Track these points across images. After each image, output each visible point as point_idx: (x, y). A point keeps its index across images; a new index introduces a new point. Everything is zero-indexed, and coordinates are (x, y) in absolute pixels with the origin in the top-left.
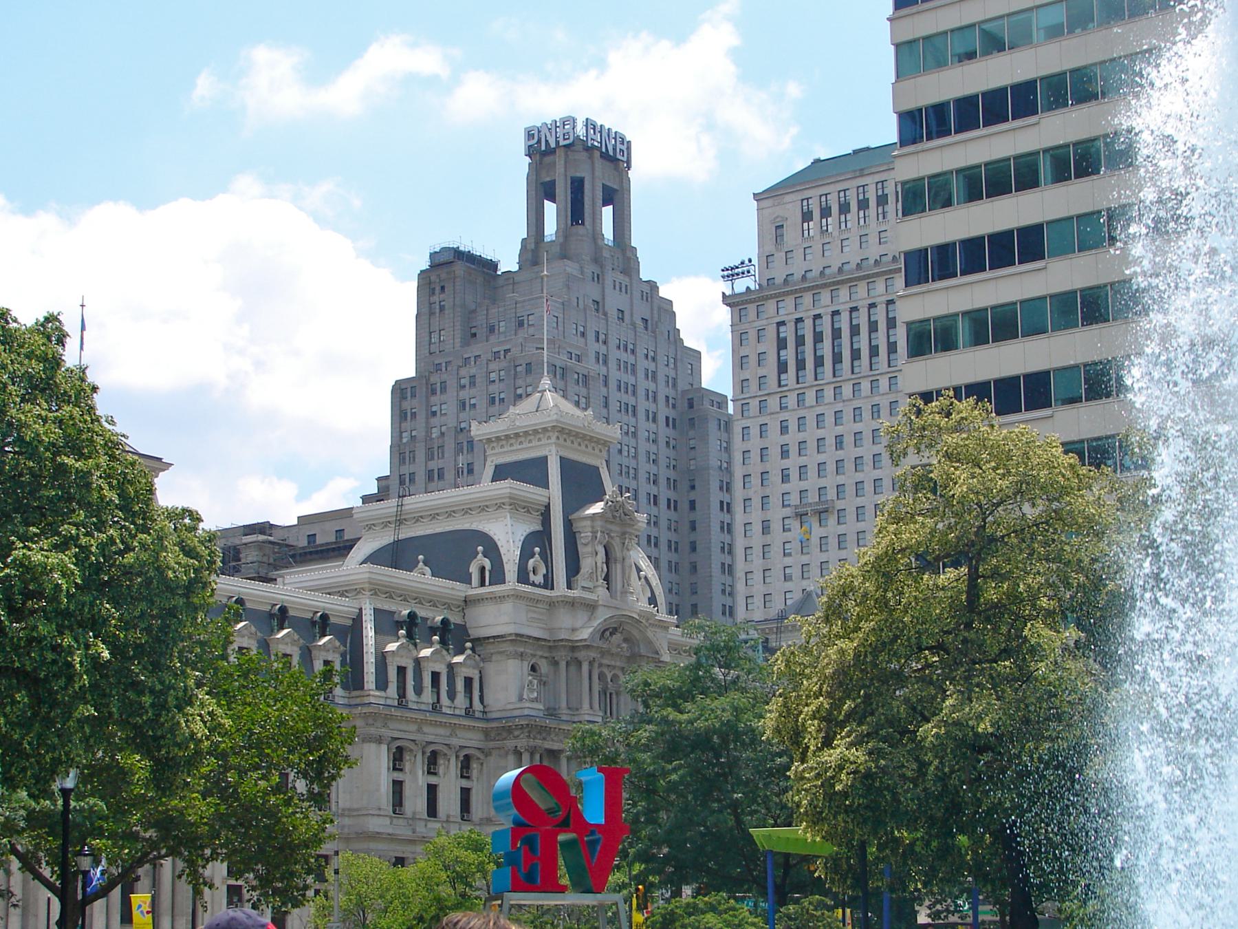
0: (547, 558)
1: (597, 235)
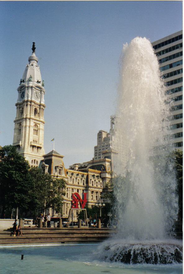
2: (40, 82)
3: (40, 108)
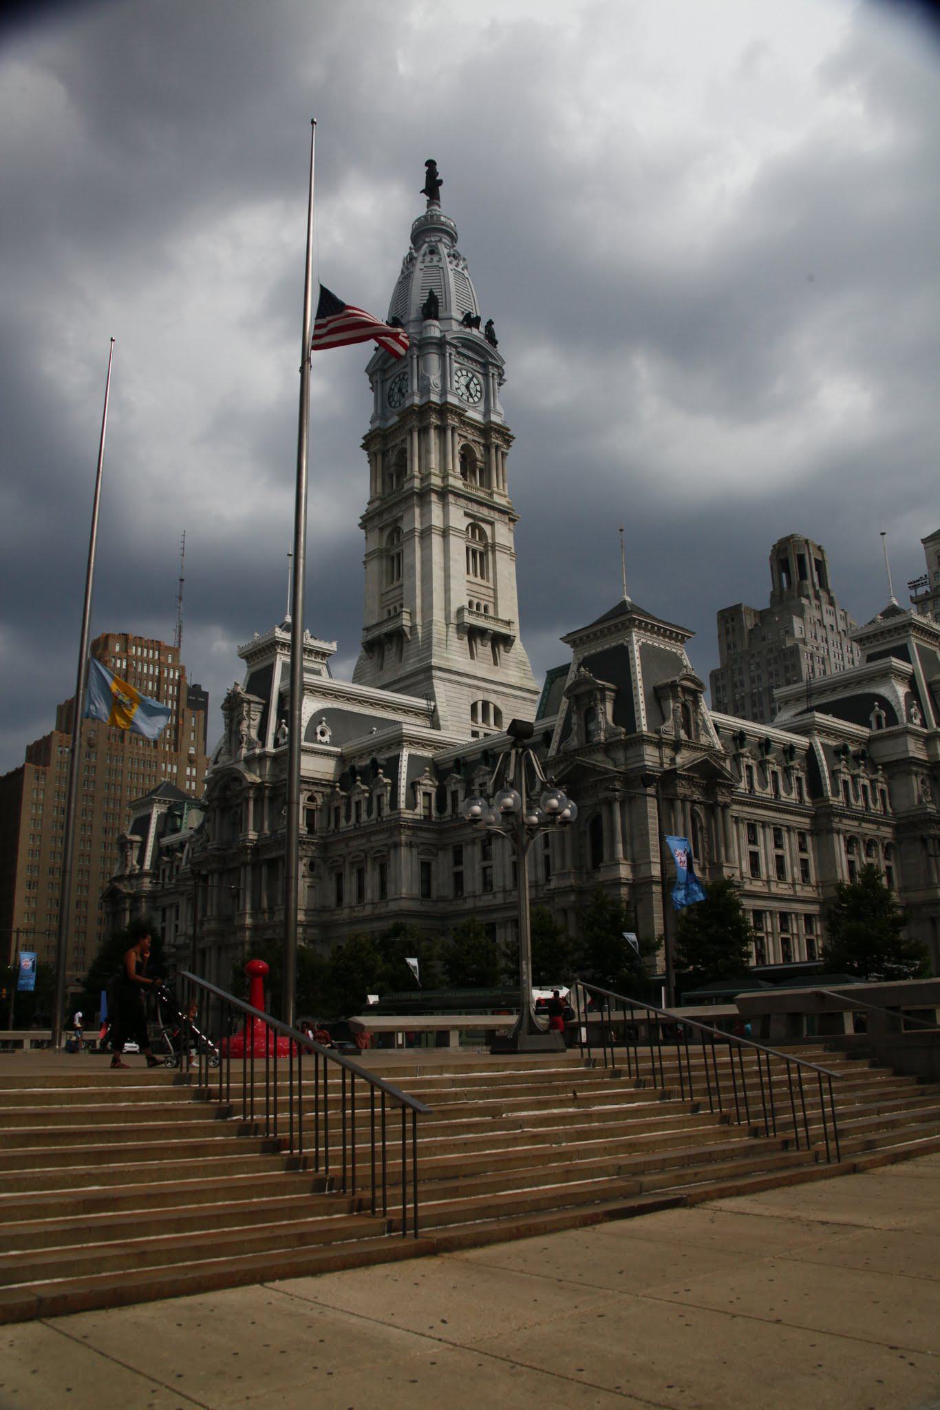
2: (478, 319)
3: (487, 448)
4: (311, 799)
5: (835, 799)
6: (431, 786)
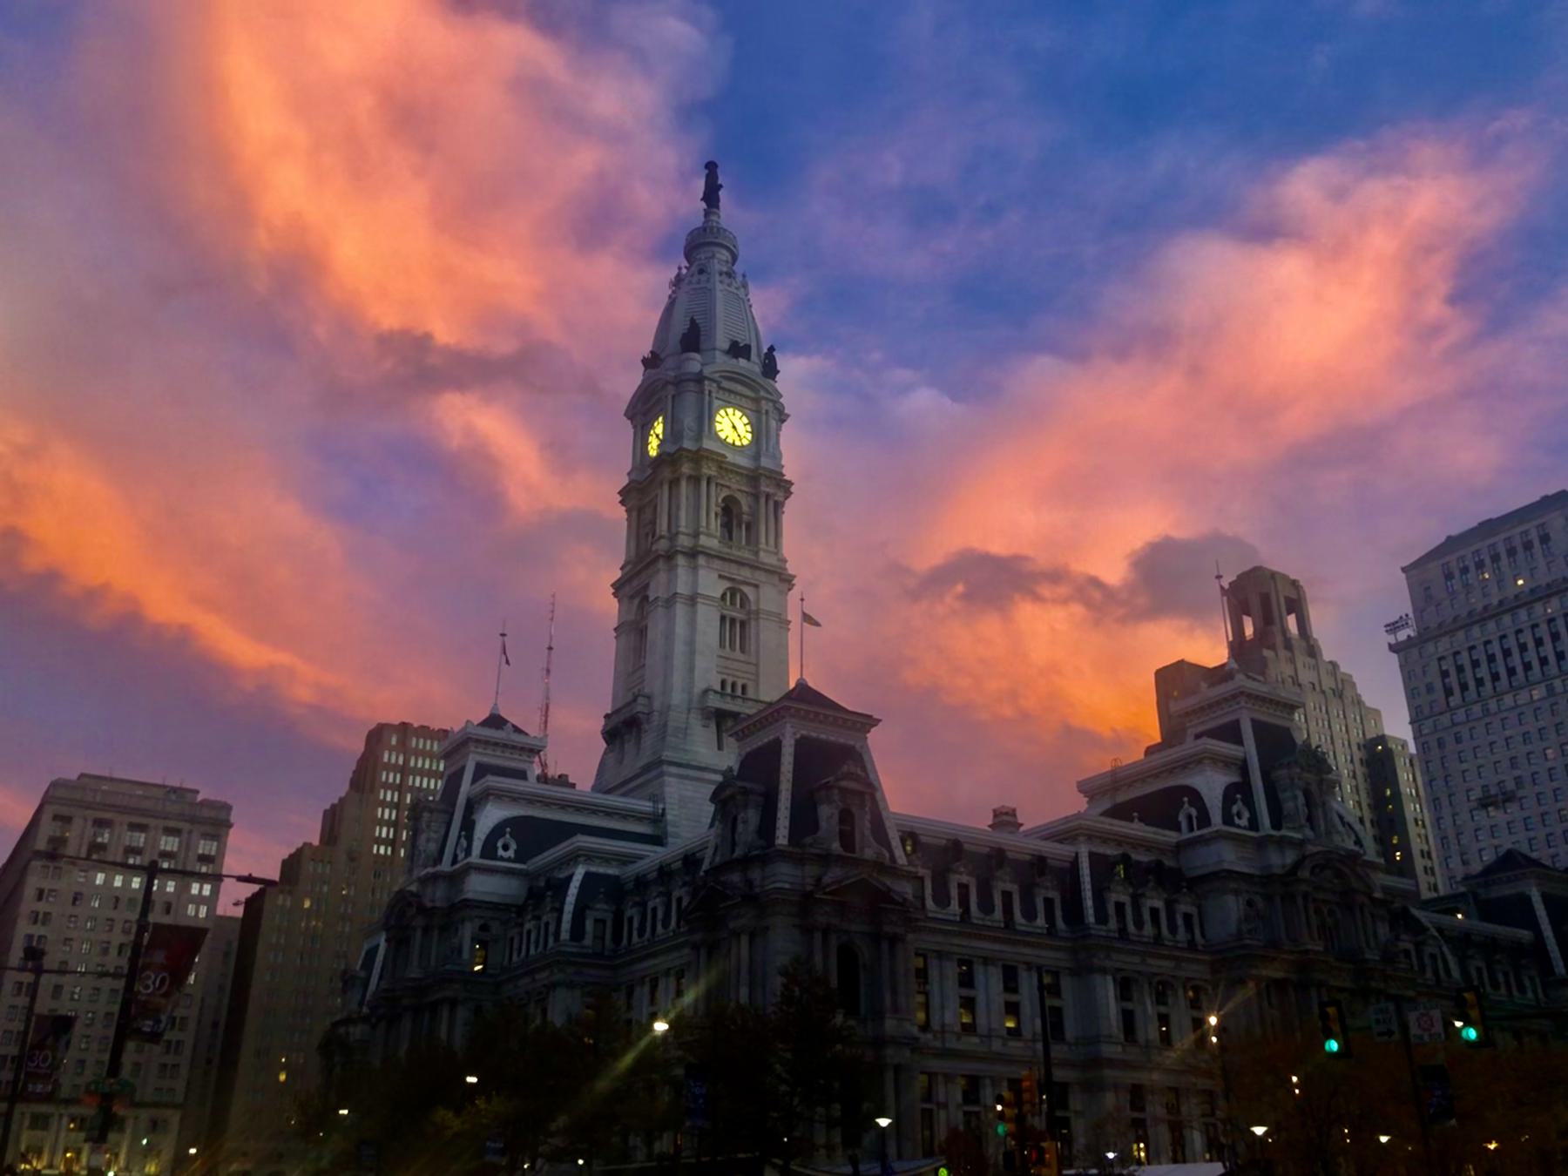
0: (1249, 803)
1: (1284, 630)
2: (748, 348)
3: (756, 497)
4: (484, 928)
5: (1104, 927)
6: (606, 911)
